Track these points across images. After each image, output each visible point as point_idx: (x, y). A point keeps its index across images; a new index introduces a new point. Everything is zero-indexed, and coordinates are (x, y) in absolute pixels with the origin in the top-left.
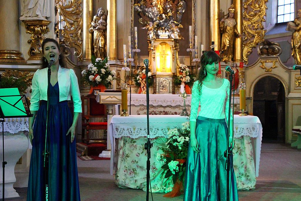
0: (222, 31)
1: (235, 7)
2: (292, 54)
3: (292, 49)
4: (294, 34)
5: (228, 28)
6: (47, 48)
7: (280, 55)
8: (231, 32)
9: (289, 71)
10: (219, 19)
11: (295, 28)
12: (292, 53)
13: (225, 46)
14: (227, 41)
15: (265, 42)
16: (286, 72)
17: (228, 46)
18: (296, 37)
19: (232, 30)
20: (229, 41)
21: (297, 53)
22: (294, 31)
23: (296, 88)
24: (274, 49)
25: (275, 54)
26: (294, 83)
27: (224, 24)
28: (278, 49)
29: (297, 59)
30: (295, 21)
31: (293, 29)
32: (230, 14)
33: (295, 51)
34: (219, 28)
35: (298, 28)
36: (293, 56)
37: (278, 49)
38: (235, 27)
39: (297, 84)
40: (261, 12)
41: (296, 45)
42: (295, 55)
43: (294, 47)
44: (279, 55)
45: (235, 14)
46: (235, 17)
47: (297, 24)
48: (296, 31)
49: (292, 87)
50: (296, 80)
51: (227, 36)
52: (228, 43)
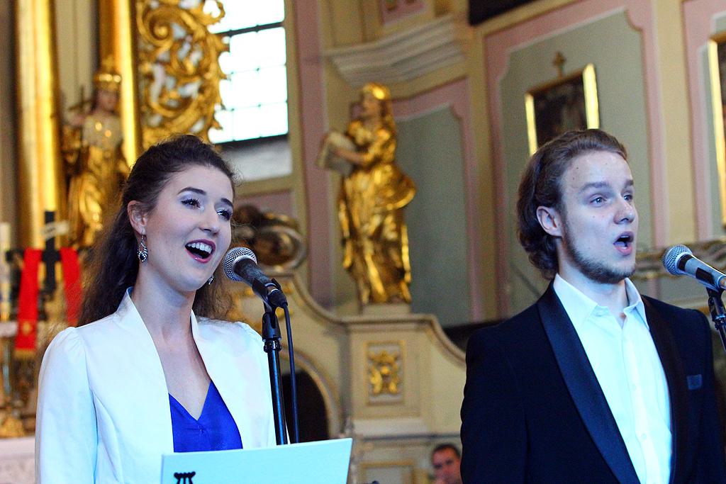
0: (71, 167)
1: (114, 72)
2: (347, 262)
3: (344, 242)
4: (349, 184)
5: (96, 155)
6: (189, 195)
7: (300, 263)
8: (105, 171)
9: (342, 329)
10: (58, 115)
11: (356, 157)
12: (343, 259)
13: (83, 227)
14: (91, 207)
15: (244, 216)
16: (325, 334)
17: (99, 227)
18: (360, 193)
19: (111, 163)
20: (102, 206)
21: (368, 259)
22: (347, 169)
23: (373, 400)
24: (275, 240)
25: (283, 260)
26: (365, 380)
27: (81, 139)
28: (293, 240)
29: (369, 285)
30: (352, 132)
31: (348, 161)
32: (105, 99)
33: (359, 250)
34: (62, 152)
35: (368, 158)
36: (351, 269)
37: (293, 240)
38: (119, 153)
39: (377, 380)
40: (208, 92)
41: (362, 224)
42: (359, 266)
43: (354, 233)
44: (296, 268)
45: (117, 95)
46: (115, 112)
47: (360, 140)
48: (356, 168)
49: (359, 395)
50: (371, 365)
51: (91, 188)
52: (96, 217)
